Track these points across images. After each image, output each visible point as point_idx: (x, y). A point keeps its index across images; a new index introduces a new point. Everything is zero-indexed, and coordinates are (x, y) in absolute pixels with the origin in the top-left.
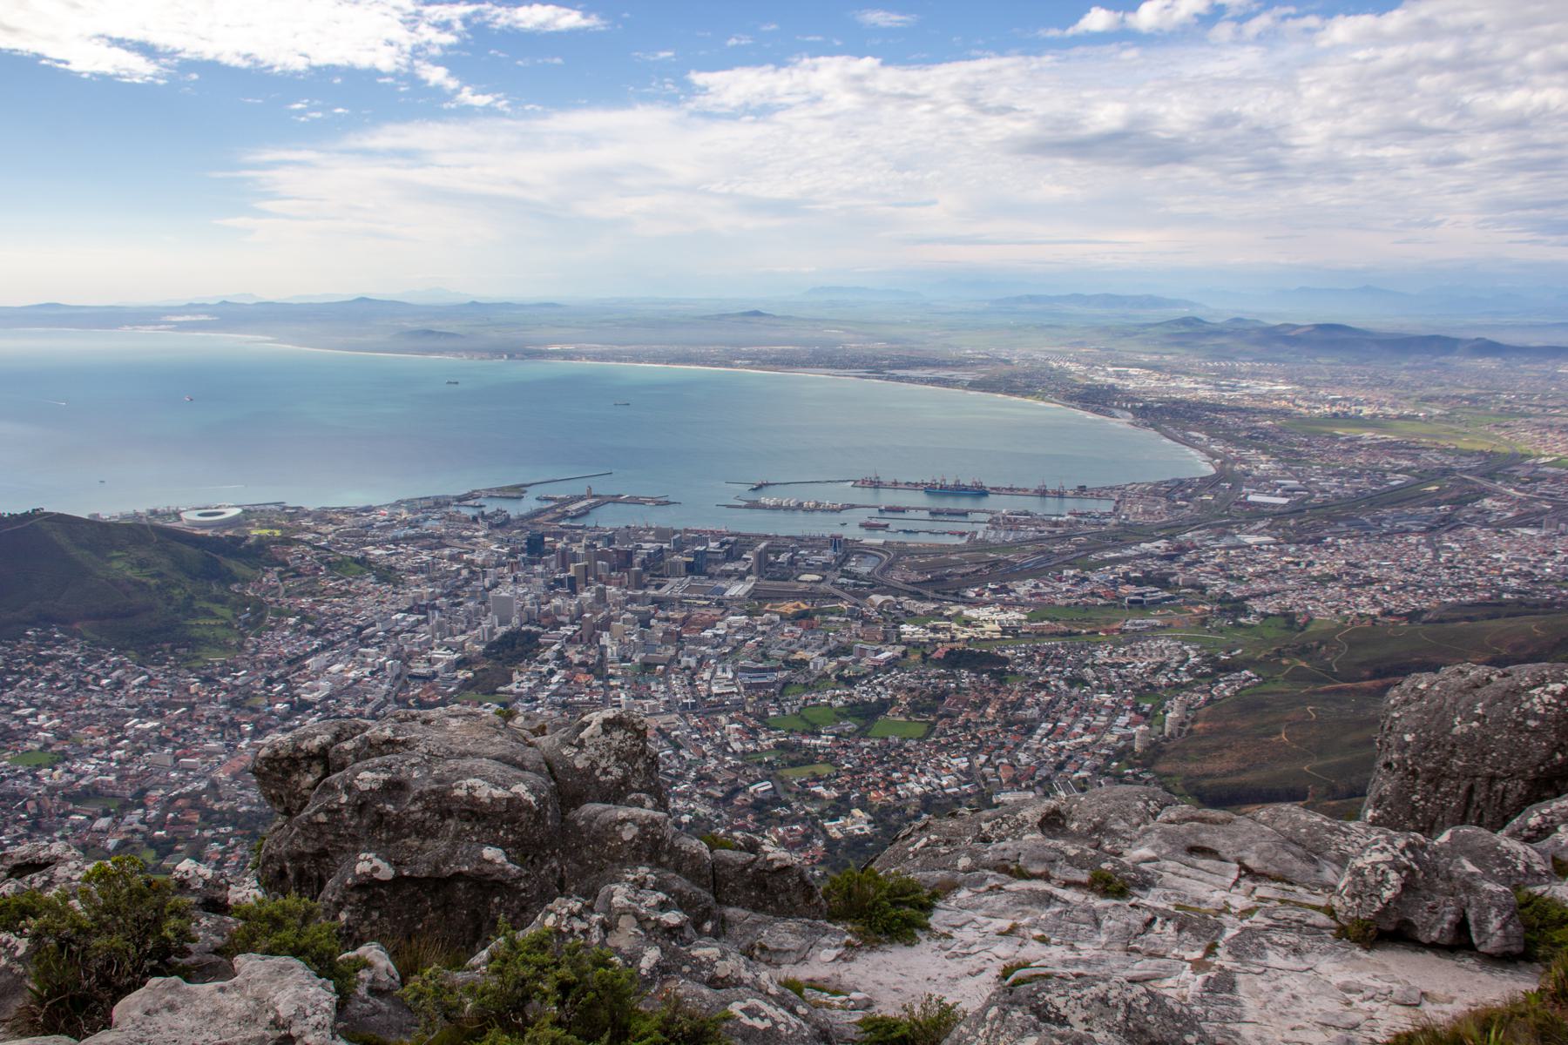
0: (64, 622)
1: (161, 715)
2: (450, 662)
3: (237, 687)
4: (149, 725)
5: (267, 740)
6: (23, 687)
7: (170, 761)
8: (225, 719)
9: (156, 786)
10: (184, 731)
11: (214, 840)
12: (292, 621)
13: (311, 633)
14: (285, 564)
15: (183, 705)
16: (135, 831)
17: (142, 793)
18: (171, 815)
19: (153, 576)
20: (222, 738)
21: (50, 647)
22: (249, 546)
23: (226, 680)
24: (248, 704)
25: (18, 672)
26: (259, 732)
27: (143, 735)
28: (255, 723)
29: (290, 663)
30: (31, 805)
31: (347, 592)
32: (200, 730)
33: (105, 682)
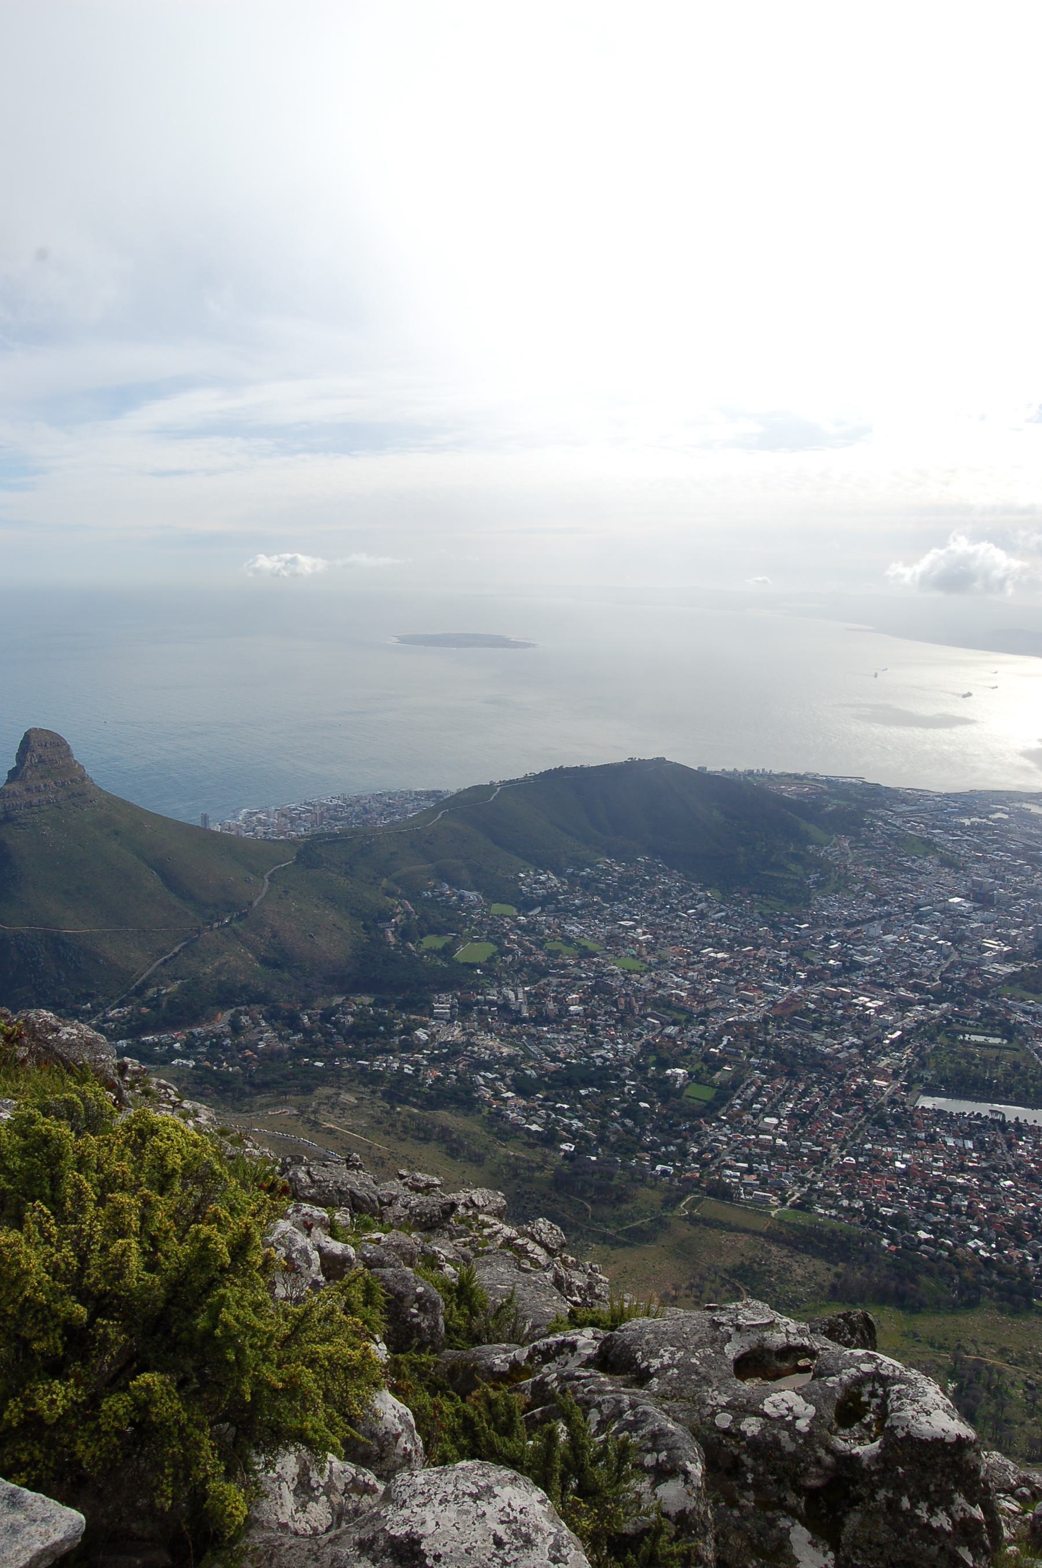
1: (729, 949)
2: (1001, 952)
4: (720, 955)
6: (629, 903)
13: (871, 902)
17: (706, 1013)
27: (713, 963)
28: (811, 974)
31: (910, 869)
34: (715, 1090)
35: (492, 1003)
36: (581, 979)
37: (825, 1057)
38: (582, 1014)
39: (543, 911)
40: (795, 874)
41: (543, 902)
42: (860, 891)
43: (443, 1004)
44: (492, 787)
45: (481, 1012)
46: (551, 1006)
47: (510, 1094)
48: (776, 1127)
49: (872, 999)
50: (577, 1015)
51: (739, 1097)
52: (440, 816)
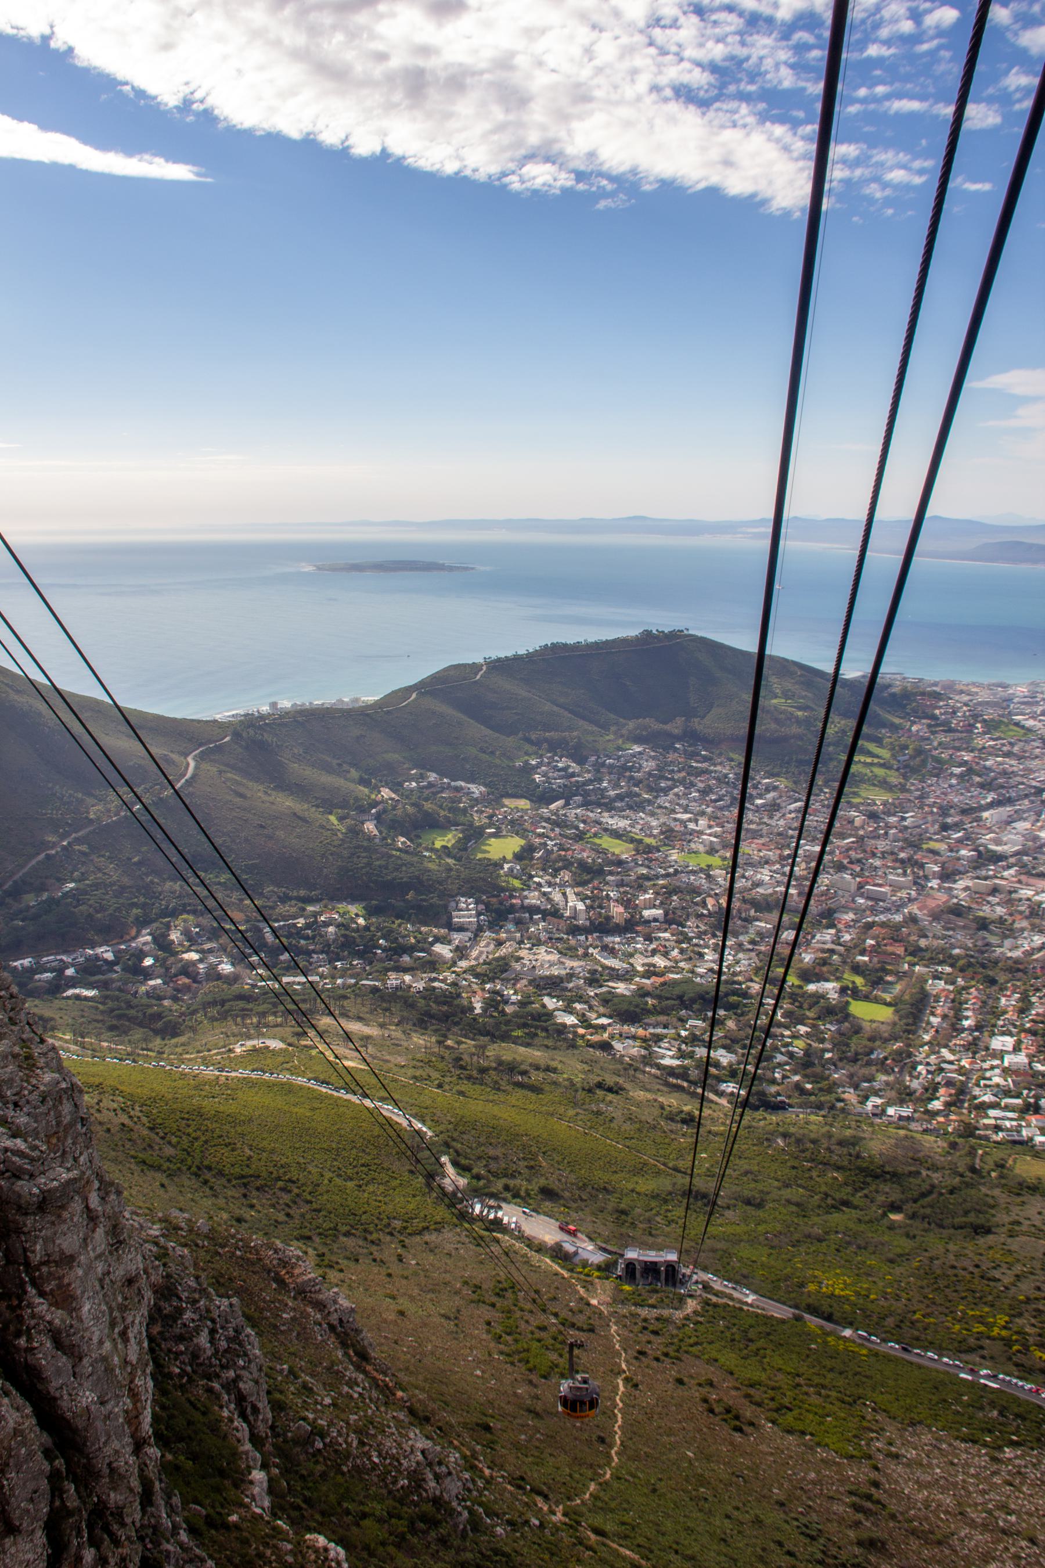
0: (709, 742)
3: (906, 828)
5: (961, 884)
6: (676, 795)
7: (853, 888)
8: (902, 855)
9: (846, 909)
10: (859, 861)
11: (937, 977)
12: (957, 771)
13: (982, 786)
14: (934, 717)
15: (851, 836)
16: (832, 952)
18: (870, 942)
19: (799, 708)
20: (905, 874)
21: (697, 762)
22: (894, 695)
23: (893, 820)
24: (925, 846)
25: (672, 779)
26: (947, 875)
29: (964, 812)
30: (710, 902)
32: (878, 863)
33: (759, 802)
34: (891, 1010)
35: (533, 910)
36: (648, 878)
37: (1017, 961)
38: (661, 919)
39: (567, 804)
40: (878, 757)
41: (567, 794)
42: (961, 776)
43: (467, 911)
44: (475, 667)
45: (518, 922)
46: (621, 909)
47: (604, 1021)
48: (1017, 1049)
49: (1037, 894)
50: (655, 920)
51: (933, 1014)
52: (414, 696)
